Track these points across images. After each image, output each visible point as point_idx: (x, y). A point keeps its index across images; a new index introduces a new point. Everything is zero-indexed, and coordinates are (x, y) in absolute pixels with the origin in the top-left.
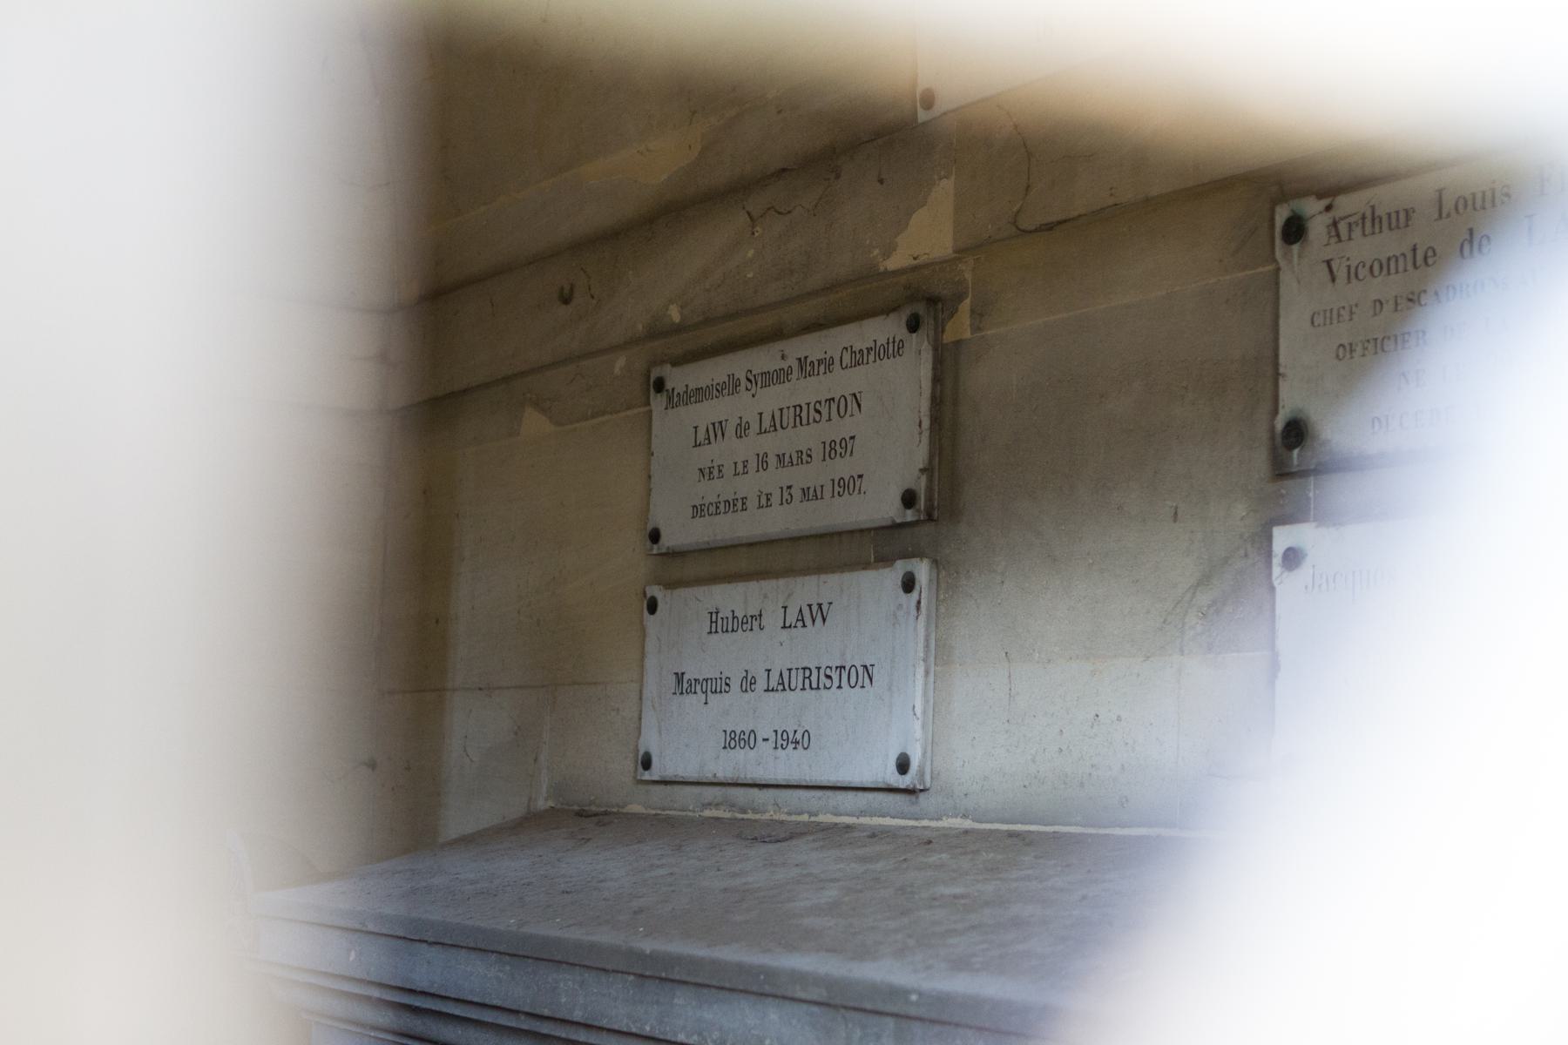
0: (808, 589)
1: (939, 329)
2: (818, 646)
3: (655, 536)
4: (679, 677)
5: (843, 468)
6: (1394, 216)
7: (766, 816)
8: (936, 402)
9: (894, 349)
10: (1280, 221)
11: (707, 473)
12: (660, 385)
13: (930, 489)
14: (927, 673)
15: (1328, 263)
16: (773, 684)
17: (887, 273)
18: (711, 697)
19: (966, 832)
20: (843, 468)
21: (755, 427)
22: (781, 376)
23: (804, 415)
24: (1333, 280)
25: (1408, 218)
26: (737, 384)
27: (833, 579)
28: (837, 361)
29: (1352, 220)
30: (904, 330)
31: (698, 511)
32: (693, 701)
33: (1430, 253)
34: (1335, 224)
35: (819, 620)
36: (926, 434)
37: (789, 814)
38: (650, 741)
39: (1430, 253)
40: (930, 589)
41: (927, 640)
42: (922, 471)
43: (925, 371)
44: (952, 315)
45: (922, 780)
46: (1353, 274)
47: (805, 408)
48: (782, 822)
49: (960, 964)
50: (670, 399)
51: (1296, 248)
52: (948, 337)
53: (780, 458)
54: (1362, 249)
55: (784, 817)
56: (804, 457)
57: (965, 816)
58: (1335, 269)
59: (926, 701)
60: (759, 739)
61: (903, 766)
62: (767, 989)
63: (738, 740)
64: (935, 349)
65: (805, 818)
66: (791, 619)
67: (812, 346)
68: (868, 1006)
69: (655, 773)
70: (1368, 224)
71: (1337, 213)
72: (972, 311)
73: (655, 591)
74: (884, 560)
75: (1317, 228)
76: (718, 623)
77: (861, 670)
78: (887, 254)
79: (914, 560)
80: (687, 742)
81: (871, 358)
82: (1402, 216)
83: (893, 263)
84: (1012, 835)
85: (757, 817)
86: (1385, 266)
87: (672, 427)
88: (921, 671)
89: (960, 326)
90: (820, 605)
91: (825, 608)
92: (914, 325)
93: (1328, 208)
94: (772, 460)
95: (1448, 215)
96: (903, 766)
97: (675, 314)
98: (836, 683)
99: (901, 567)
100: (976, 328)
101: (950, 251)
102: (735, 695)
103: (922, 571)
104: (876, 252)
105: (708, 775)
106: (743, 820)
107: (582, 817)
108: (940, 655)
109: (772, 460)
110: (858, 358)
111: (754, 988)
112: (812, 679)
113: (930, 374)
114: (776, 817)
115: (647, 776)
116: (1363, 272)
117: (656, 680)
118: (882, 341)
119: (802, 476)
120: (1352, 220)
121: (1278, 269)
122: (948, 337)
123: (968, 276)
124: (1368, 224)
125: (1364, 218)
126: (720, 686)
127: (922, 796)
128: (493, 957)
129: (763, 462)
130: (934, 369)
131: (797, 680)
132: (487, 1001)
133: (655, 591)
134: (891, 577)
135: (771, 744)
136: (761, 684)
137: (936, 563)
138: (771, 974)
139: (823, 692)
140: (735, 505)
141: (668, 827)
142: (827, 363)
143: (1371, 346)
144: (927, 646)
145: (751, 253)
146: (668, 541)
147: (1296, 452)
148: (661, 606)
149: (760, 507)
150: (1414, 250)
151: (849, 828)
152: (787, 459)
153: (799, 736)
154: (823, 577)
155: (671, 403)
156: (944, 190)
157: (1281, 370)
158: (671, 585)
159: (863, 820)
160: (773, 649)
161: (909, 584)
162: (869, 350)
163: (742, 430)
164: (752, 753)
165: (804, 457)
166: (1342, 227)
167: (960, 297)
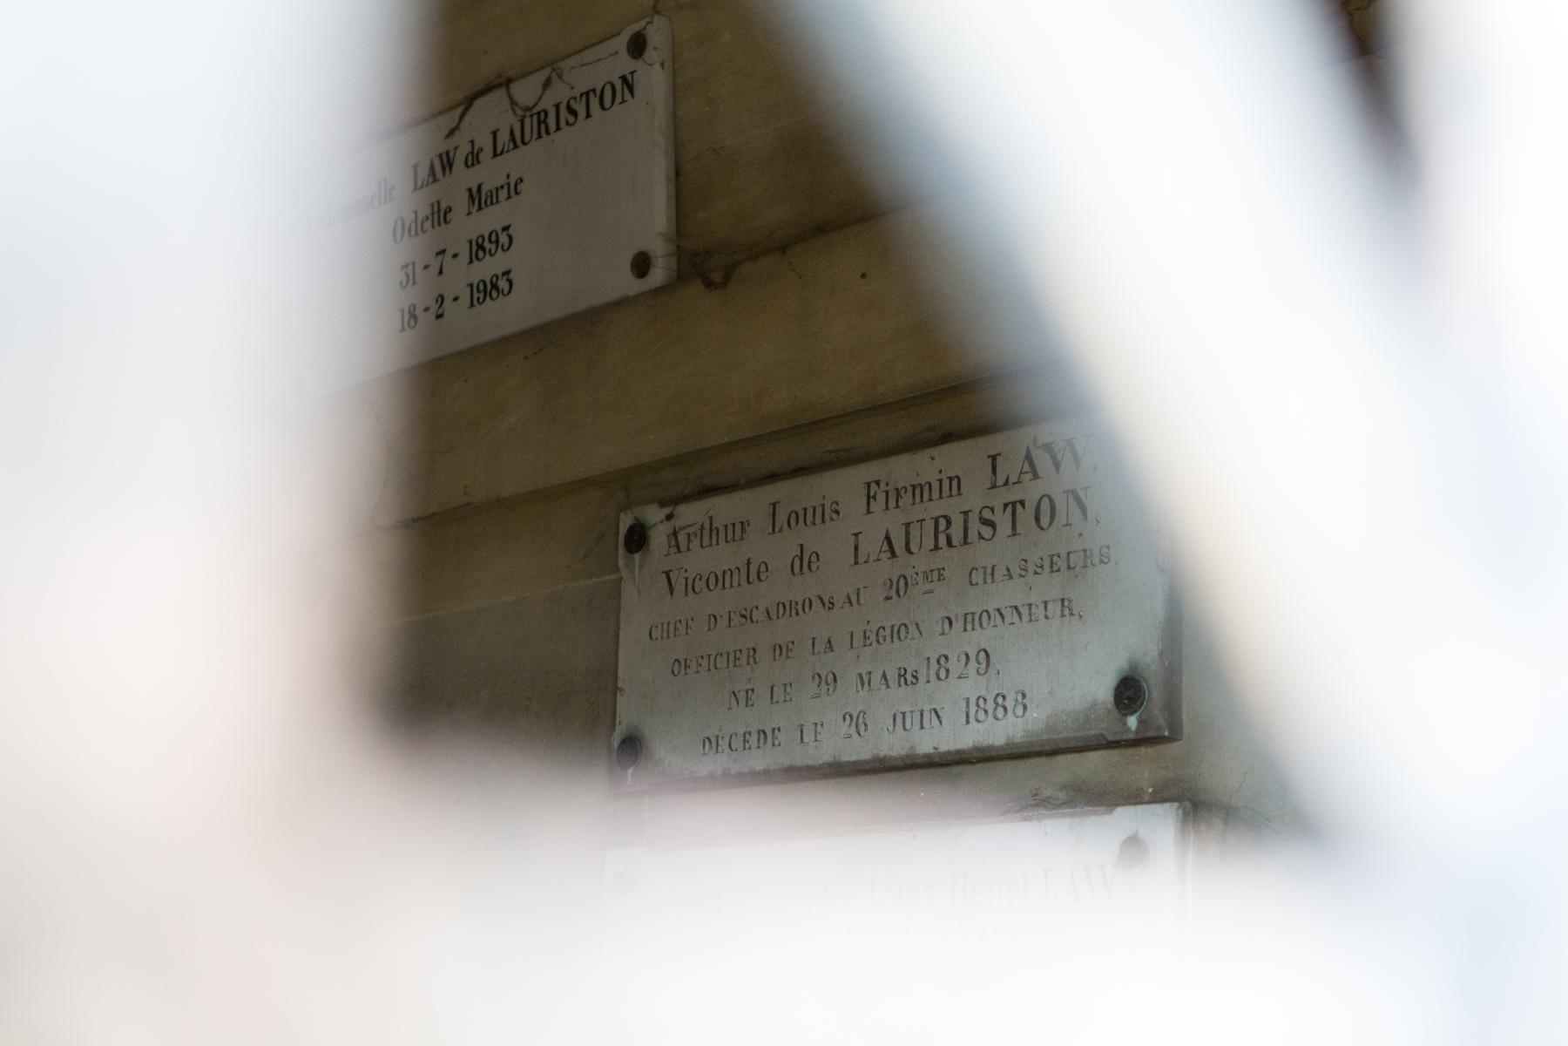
10: (623, 529)
15: (667, 574)
29: (691, 530)
33: (763, 568)
34: (675, 534)
39: (763, 568)
46: (690, 587)
51: (637, 556)
54: (702, 560)
70: (706, 532)
71: (678, 522)
75: (658, 538)
86: (720, 580)
93: (669, 517)
95: (781, 530)
120: (691, 530)
124: (706, 532)
125: (702, 529)
143: (704, 663)
150: (748, 564)
157: (620, 684)
166: (682, 537)
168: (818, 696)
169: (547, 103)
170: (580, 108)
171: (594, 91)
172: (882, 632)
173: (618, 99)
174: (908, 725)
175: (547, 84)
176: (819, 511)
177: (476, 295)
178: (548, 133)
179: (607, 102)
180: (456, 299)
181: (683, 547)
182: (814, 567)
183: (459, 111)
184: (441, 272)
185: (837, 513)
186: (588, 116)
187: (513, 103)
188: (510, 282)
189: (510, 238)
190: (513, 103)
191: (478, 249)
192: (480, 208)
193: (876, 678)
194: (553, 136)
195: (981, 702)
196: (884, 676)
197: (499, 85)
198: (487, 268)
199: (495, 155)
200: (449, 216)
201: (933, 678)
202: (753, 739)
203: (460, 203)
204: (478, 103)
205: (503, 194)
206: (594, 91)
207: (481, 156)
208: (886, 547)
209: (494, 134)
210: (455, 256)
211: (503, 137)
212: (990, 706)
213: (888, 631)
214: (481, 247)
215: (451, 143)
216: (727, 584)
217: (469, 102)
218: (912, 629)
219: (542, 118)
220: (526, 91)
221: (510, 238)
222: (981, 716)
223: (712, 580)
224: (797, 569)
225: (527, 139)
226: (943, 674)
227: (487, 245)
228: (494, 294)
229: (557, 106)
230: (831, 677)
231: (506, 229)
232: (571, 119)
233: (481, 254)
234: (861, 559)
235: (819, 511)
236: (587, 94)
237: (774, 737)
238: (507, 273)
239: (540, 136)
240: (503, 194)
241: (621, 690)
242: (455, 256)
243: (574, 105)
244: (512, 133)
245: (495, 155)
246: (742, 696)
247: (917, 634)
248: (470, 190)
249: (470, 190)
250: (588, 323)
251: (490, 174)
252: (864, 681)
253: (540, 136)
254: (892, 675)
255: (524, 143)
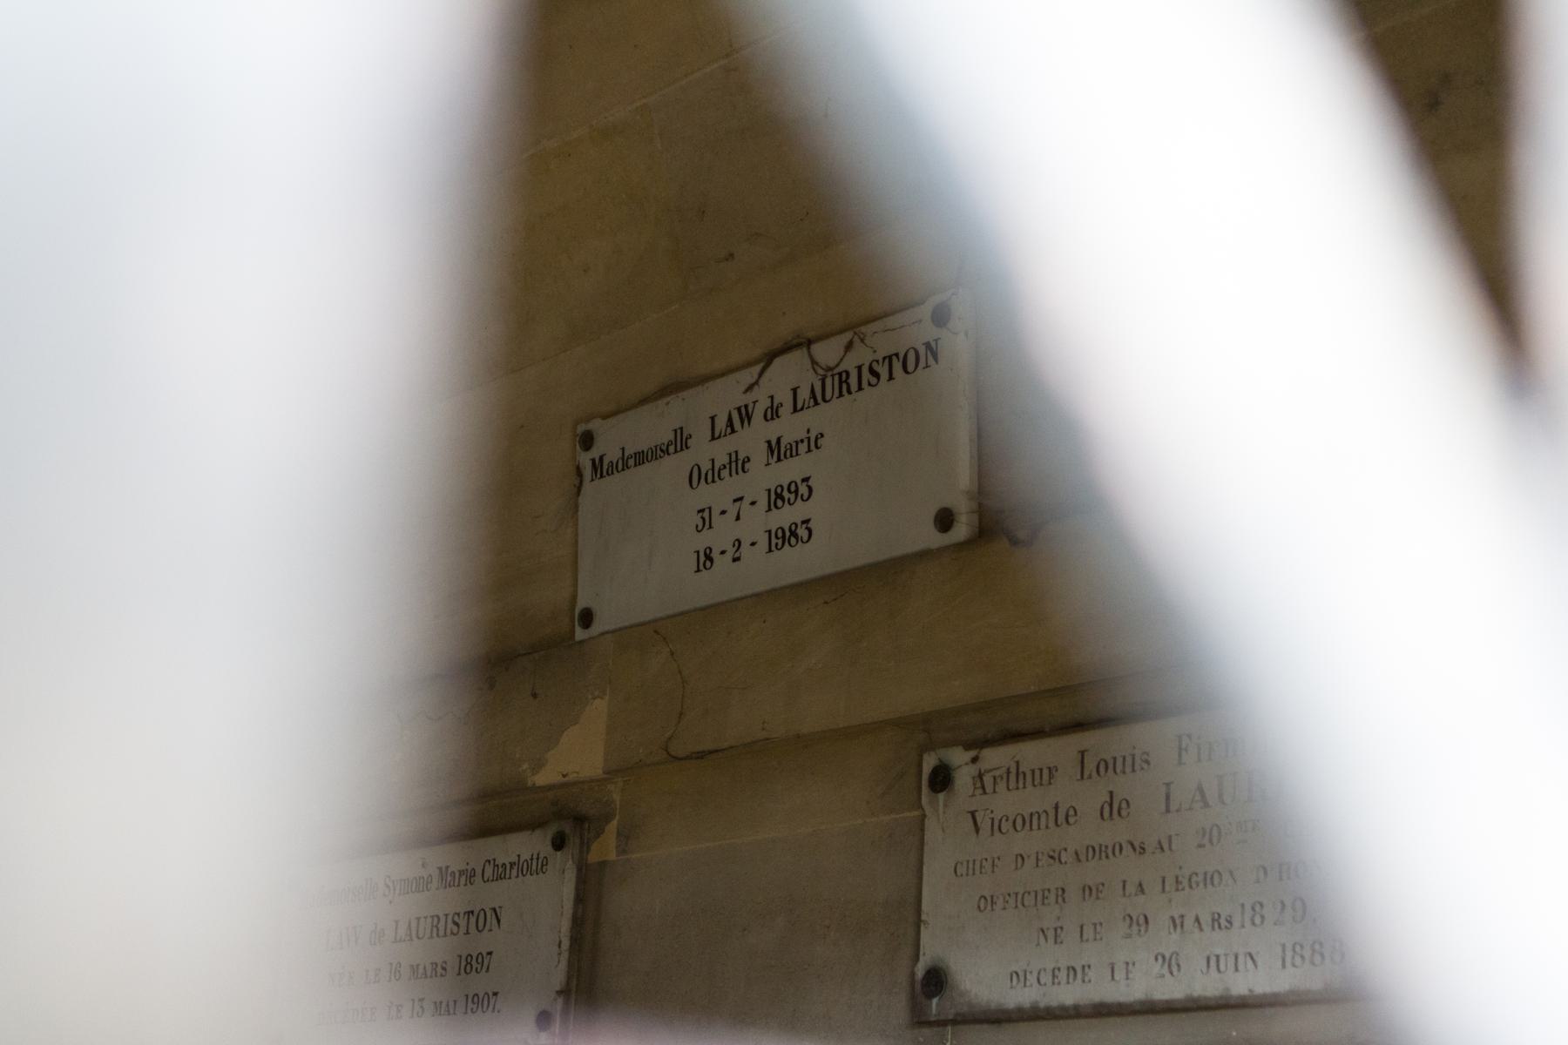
1: (585, 846)
6: (1037, 773)
8: (578, 922)
9: (536, 866)
10: (927, 768)
15: (973, 814)
24: (977, 831)
25: (1051, 776)
28: (479, 872)
29: (997, 773)
30: (550, 848)
34: (980, 776)
36: (565, 955)
42: (559, 993)
44: (598, 835)
46: (996, 827)
51: (941, 796)
52: (593, 857)
54: (1005, 803)
58: (979, 820)
64: (579, 870)
70: (1013, 777)
71: (984, 765)
72: (619, 834)
75: (963, 779)
81: (514, 872)
82: (1046, 772)
83: (542, 779)
86: (1027, 821)
89: (606, 847)
92: (559, 843)
93: (975, 760)
100: (622, 851)
104: (525, 766)
113: (572, 896)
116: (1029, 900)
118: (526, 856)
120: (997, 773)
121: (924, 816)
122: (593, 857)
123: (617, 797)
124: (1013, 777)
125: (1008, 772)
130: (577, 889)
143: (1012, 901)
147: (935, 1001)
150: (1056, 808)
152: (421, 970)
156: (598, 708)
157: (924, 917)
162: (512, 865)
166: (988, 779)
167: (608, 818)
168: (1129, 936)
169: (850, 364)
170: (883, 370)
171: (897, 355)
172: (1194, 879)
173: (922, 364)
174: (1222, 967)
175: (849, 347)
176: (1129, 760)
177: (774, 541)
178: (849, 392)
179: (910, 368)
180: (753, 544)
181: (989, 789)
182: (1124, 813)
183: (758, 368)
184: (738, 518)
185: (1147, 762)
186: (891, 378)
187: (814, 362)
188: (810, 531)
189: (810, 489)
190: (814, 362)
191: (777, 498)
192: (779, 460)
193: (1189, 922)
194: (854, 395)
195: (1298, 948)
196: (1197, 920)
197: (799, 345)
198: (786, 516)
199: (795, 410)
200: (747, 466)
201: (1248, 923)
202: (1062, 975)
203: (759, 455)
204: (777, 362)
205: (803, 448)
206: (897, 355)
207: (781, 411)
208: (1198, 798)
209: (795, 391)
210: (753, 503)
211: (804, 394)
212: (1307, 953)
213: (1201, 878)
214: (779, 496)
215: (748, 399)
216: (1035, 826)
217: (770, 358)
218: (1226, 876)
219: (843, 378)
220: (828, 352)
221: (810, 489)
222: (1298, 960)
223: (1019, 821)
224: (1106, 814)
225: (828, 396)
226: (1258, 920)
227: (786, 494)
228: (793, 540)
229: (859, 368)
230: (1142, 920)
231: (805, 480)
232: (874, 380)
233: (779, 503)
234: (1173, 807)
235: (1129, 760)
236: (890, 358)
237: (1084, 973)
238: (807, 521)
239: (841, 395)
240: (803, 448)
241: (926, 923)
242: (753, 503)
243: (875, 366)
244: (813, 391)
245: (795, 410)
246: (1050, 934)
247: (1230, 881)
248: (769, 442)
249: (769, 442)
250: (889, 572)
251: (789, 428)
252: (1177, 923)
253: (841, 395)
254: (1206, 919)
255: (824, 400)
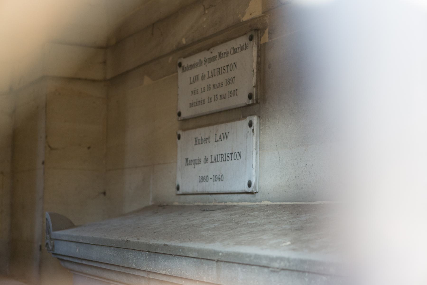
0: (222, 128)
1: (259, 39)
2: (226, 147)
3: (179, 114)
4: (187, 159)
5: (231, 87)
7: (212, 204)
9: (245, 47)
11: (194, 92)
12: (180, 65)
13: (257, 93)
14: (257, 154)
16: (213, 160)
17: (243, 22)
18: (197, 166)
19: (268, 205)
20: (231, 87)
21: (207, 76)
22: (213, 59)
23: (220, 71)
26: (201, 63)
27: (229, 124)
30: (248, 41)
31: (191, 105)
32: (191, 167)
35: (225, 138)
36: (255, 74)
37: (219, 203)
38: (179, 181)
40: (257, 125)
41: (256, 142)
42: (254, 87)
43: (255, 53)
44: (263, 34)
45: (256, 190)
47: (221, 68)
48: (216, 205)
49: (239, 243)
50: (183, 69)
52: (262, 42)
53: (214, 86)
55: (217, 204)
56: (220, 85)
57: (268, 200)
59: (257, 163)
60: (209, 178)
61: (250, 185)
62: (182, 254)
63: (204, 179)
64: (258, 46)
65: (223, 204)
66: (218, 139)
67: (222, 48)
68: (209, 258)
69: (180, 192)
72: (269, 33)
73: (180, 132)
74: (244, 117)
76: (198, 142)
77: (237, 154)
78: (243, 16)
79: (252, 116)
80: (189, 181)
81: (239, 50)
83: (246, 18)
84: (280, 205)
85: (210, 204)
87: (184, 78)
88: (254, 153)
89: (265, 38)
90: (226, 133)
91: (227, 134)
92: (251, 39)
94: (212, 87)
96: (250, 185)
97: (184, 41)
98: (230, 159)
99: (248, 119)
100: (270, 38)
101: (261, 13)
102: (202, 165)
103: (255, 120)
104: (240, 15)
105: (195, 191)
106: (207, 205)
107: (161, 207)
108: (261, 147)
109: (212, 87)
110: (235, 51)
111: (178, 254)
112: (224, 157)
114: (215, 204)
115: (178, 192)
117: (180, 161)
118: (242, 45)
119: (220, 91)
122: (262, 42)
126: (197, 162)
127: (256, 194)
128: (112, 248)
129: (209, 88)
130: (258, 53)
131: (219, 158)
132: (111, 263)
133: (180, 132)
134: (246, 122)
135: (212, 180)
136: (210, 160)
137: (259, 117)
138: (183, 249)
139: (227, 162)
140: (201, 102)
141: (182, 209)
142: (227, 53)
144: (256, 145)
145: (205, 19)
146: (184, 115)
148: (182, 137)
149: (209, 102)
151: (234, 206)
153: (220, 177)
154: (227, 124)
155: (183, 71)
158: (184, 130)
159: (240, 204)
160: (213, 149)
161: (250, 125)
162: (238, 48)
163: (203, 77)
164: (207, 183)
165: (220, 85)
167: (265, 28)
